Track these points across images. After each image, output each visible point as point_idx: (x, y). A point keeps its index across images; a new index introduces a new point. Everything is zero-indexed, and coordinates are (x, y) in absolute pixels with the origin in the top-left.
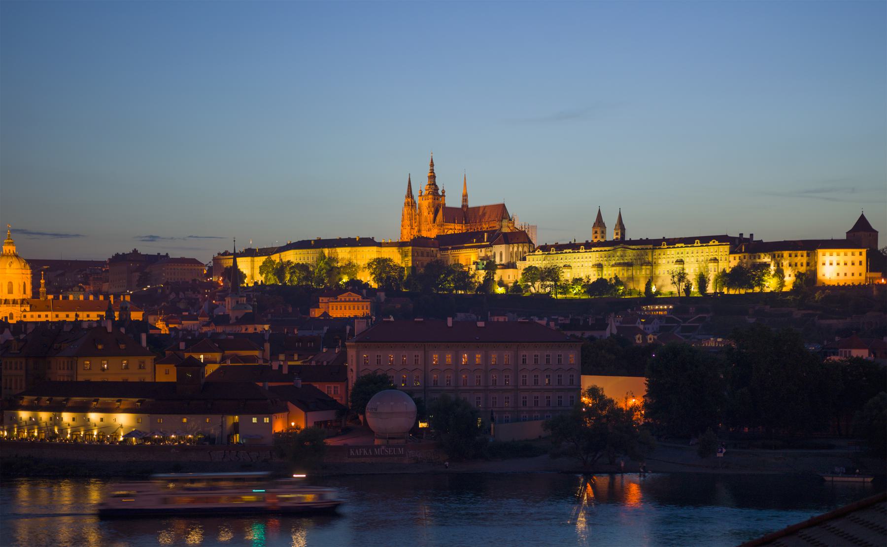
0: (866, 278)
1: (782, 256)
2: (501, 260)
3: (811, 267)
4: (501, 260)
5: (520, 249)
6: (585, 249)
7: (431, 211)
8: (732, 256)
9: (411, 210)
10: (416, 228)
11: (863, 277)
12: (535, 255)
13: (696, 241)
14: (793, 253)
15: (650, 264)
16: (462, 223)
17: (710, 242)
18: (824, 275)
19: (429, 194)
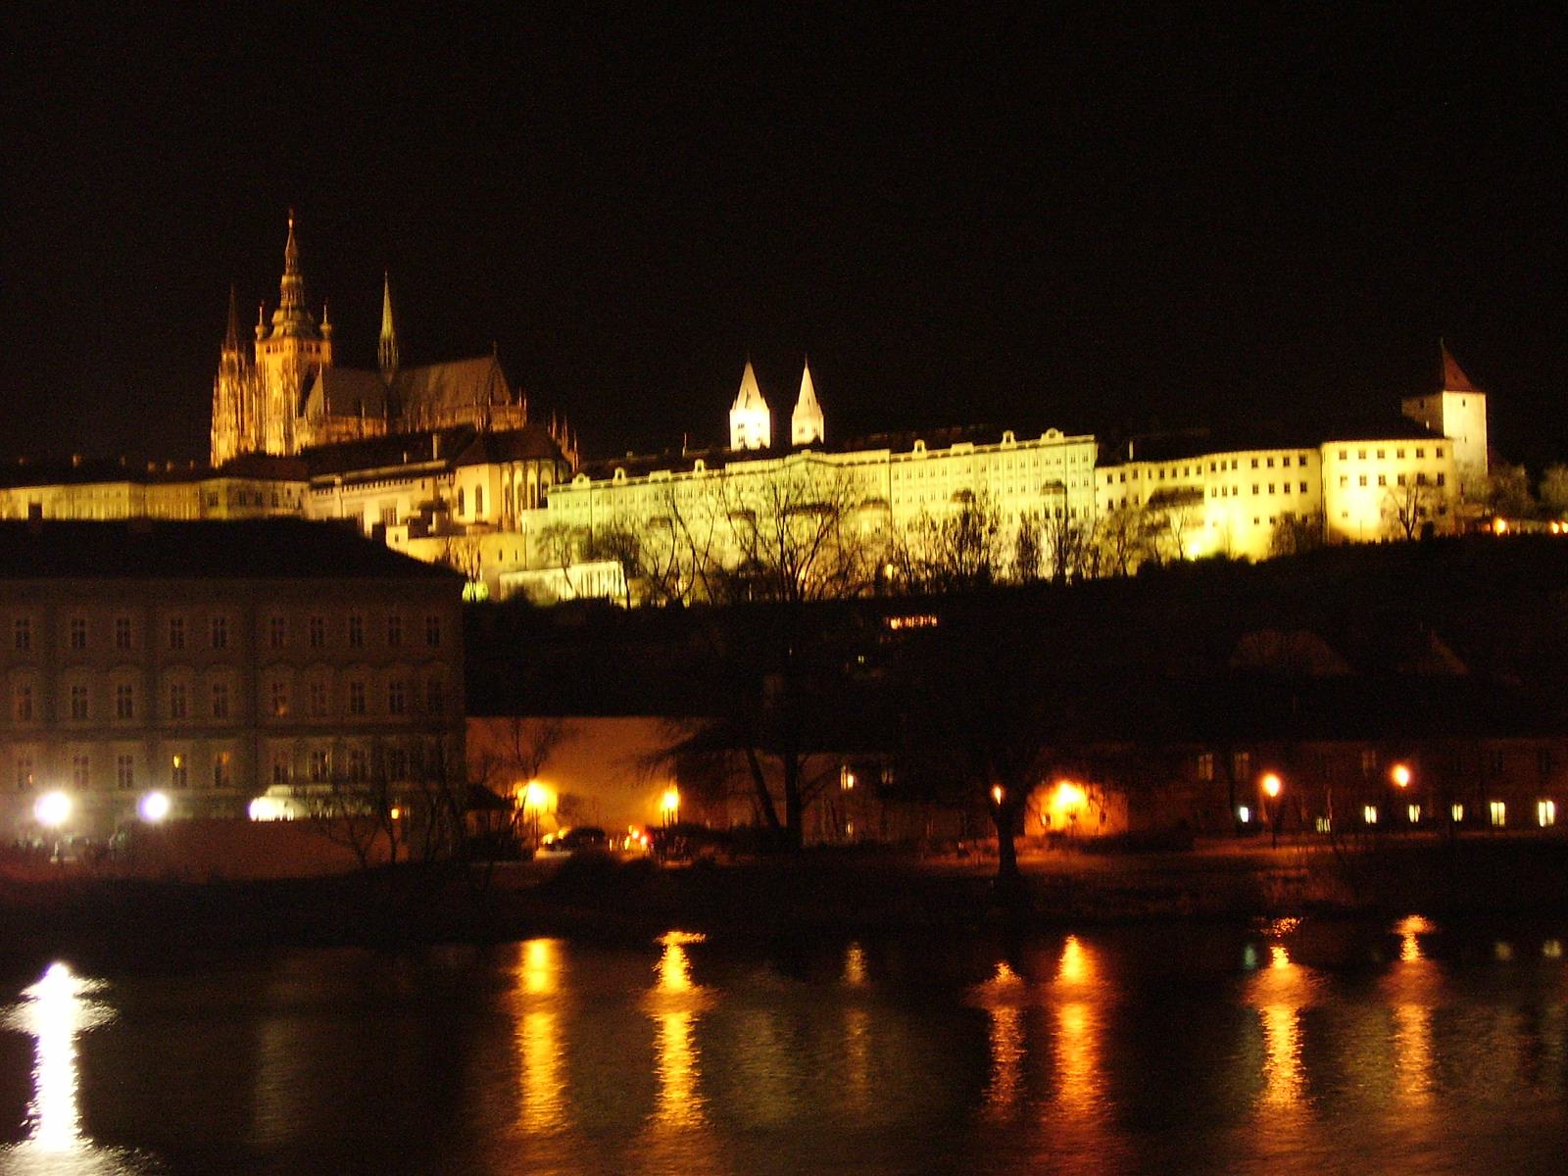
2: (479, 509)
4: (479, 509)
5: (532, 477)
7: (290, 383)
8: (1102, 473)
9: (240, 384)
17: (1043, 436)
18: (1345, 515)
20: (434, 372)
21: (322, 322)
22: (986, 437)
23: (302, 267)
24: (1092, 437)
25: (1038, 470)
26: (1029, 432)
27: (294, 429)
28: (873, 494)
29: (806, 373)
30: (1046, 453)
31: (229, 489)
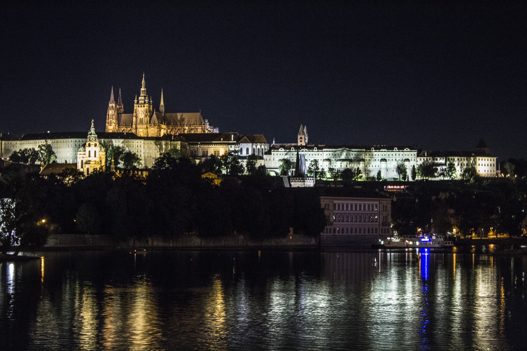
0: (497, 174)
1: (454, 160)
2: (247, 152)
3: (469, 166)
4: (247, 152)
5: (263, 147)
6: (317, 149)
8: (418, 159)
10: (117, 125)
11: (495, 173)
12: (278, 151)
13: (395, 148)
14: (460, 158)
15: (363, 160)
16: (165, 124)
18: (479, 171)
19: (145, 103)
20: (179, 115)
21: (150, 100)
22: (390, 148)
23: (146, 87)
24: (416, 151)
25: (403, 156)
26: (401, 148)
27: (148, 126)
28: (361, 158)
29: (305, 126)
30: (405, 153)
31: (181, 143)
